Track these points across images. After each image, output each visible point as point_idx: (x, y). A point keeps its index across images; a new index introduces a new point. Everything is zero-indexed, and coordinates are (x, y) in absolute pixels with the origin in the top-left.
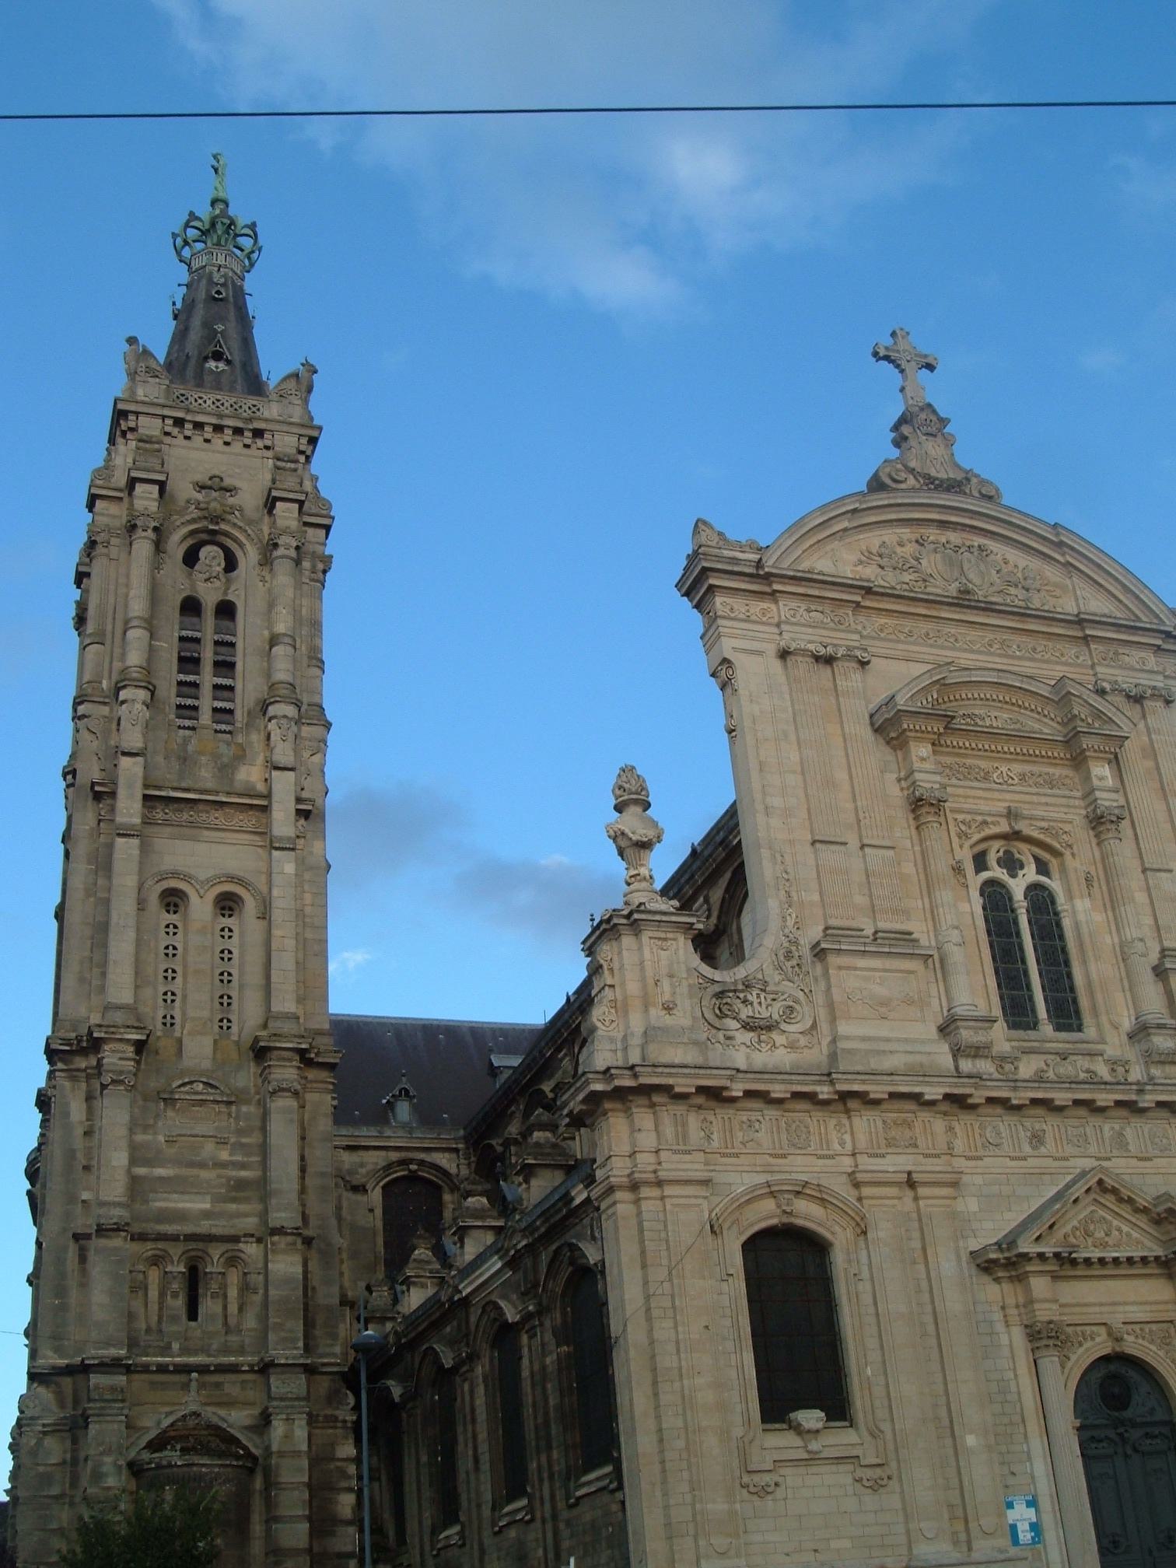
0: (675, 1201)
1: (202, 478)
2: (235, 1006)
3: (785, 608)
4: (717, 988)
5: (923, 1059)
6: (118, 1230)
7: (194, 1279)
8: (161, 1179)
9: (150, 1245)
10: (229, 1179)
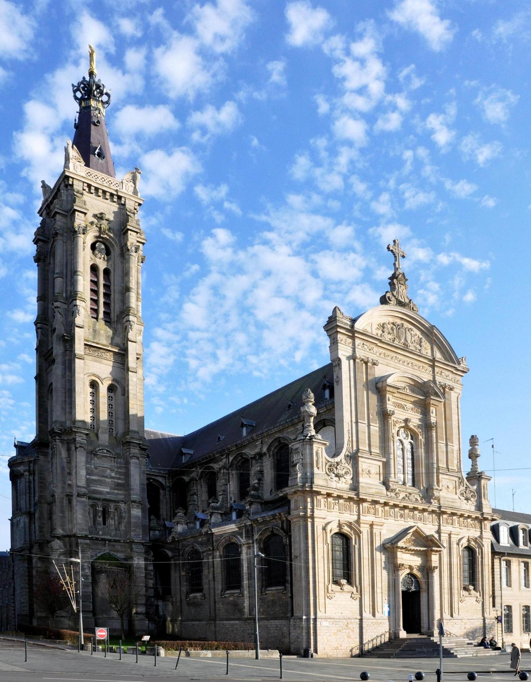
2: (114, 425)
7: (105, 513)
8: (93, 479)
10: (115, 482)
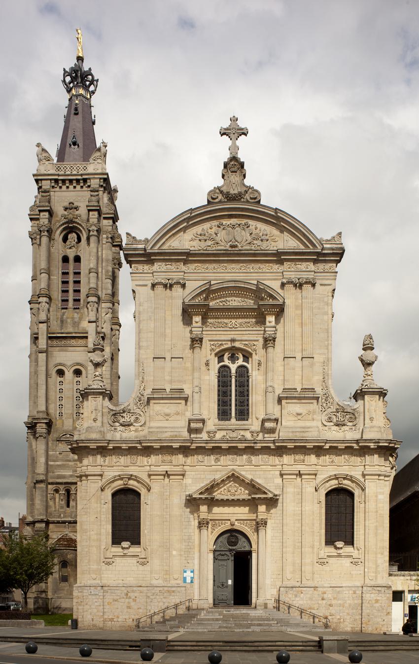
0: (91, 481)
1: (66, 204)
3: (156, 266)
4: (114, 412)
5: (177, 434)
6: (42, 482)
9: (55, 486)
